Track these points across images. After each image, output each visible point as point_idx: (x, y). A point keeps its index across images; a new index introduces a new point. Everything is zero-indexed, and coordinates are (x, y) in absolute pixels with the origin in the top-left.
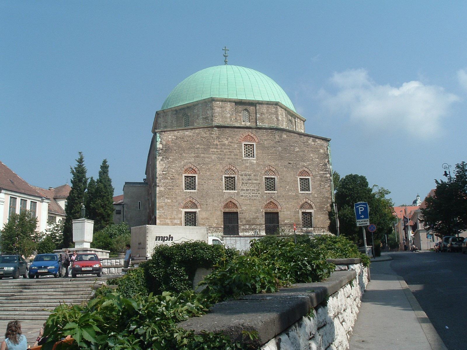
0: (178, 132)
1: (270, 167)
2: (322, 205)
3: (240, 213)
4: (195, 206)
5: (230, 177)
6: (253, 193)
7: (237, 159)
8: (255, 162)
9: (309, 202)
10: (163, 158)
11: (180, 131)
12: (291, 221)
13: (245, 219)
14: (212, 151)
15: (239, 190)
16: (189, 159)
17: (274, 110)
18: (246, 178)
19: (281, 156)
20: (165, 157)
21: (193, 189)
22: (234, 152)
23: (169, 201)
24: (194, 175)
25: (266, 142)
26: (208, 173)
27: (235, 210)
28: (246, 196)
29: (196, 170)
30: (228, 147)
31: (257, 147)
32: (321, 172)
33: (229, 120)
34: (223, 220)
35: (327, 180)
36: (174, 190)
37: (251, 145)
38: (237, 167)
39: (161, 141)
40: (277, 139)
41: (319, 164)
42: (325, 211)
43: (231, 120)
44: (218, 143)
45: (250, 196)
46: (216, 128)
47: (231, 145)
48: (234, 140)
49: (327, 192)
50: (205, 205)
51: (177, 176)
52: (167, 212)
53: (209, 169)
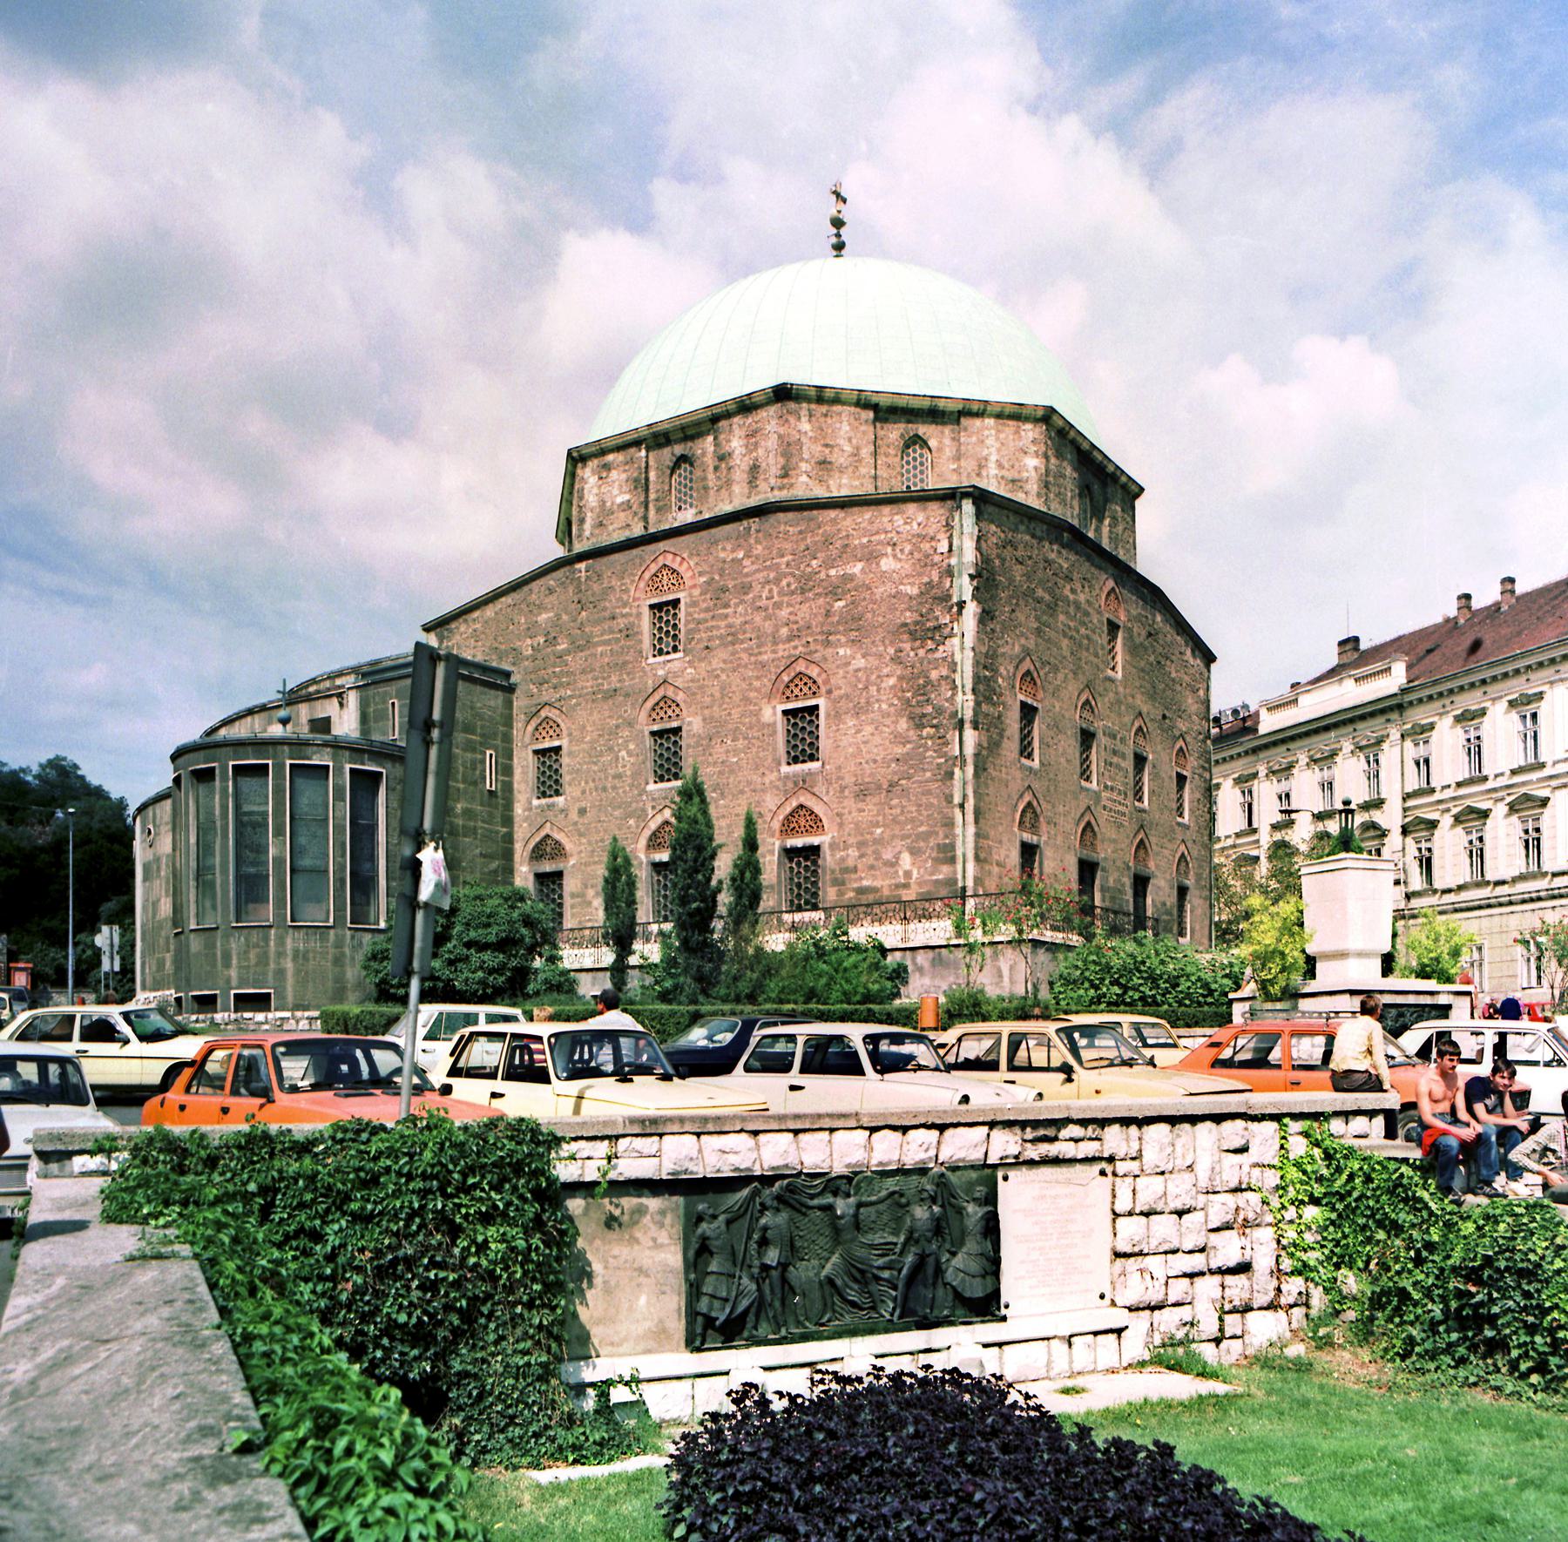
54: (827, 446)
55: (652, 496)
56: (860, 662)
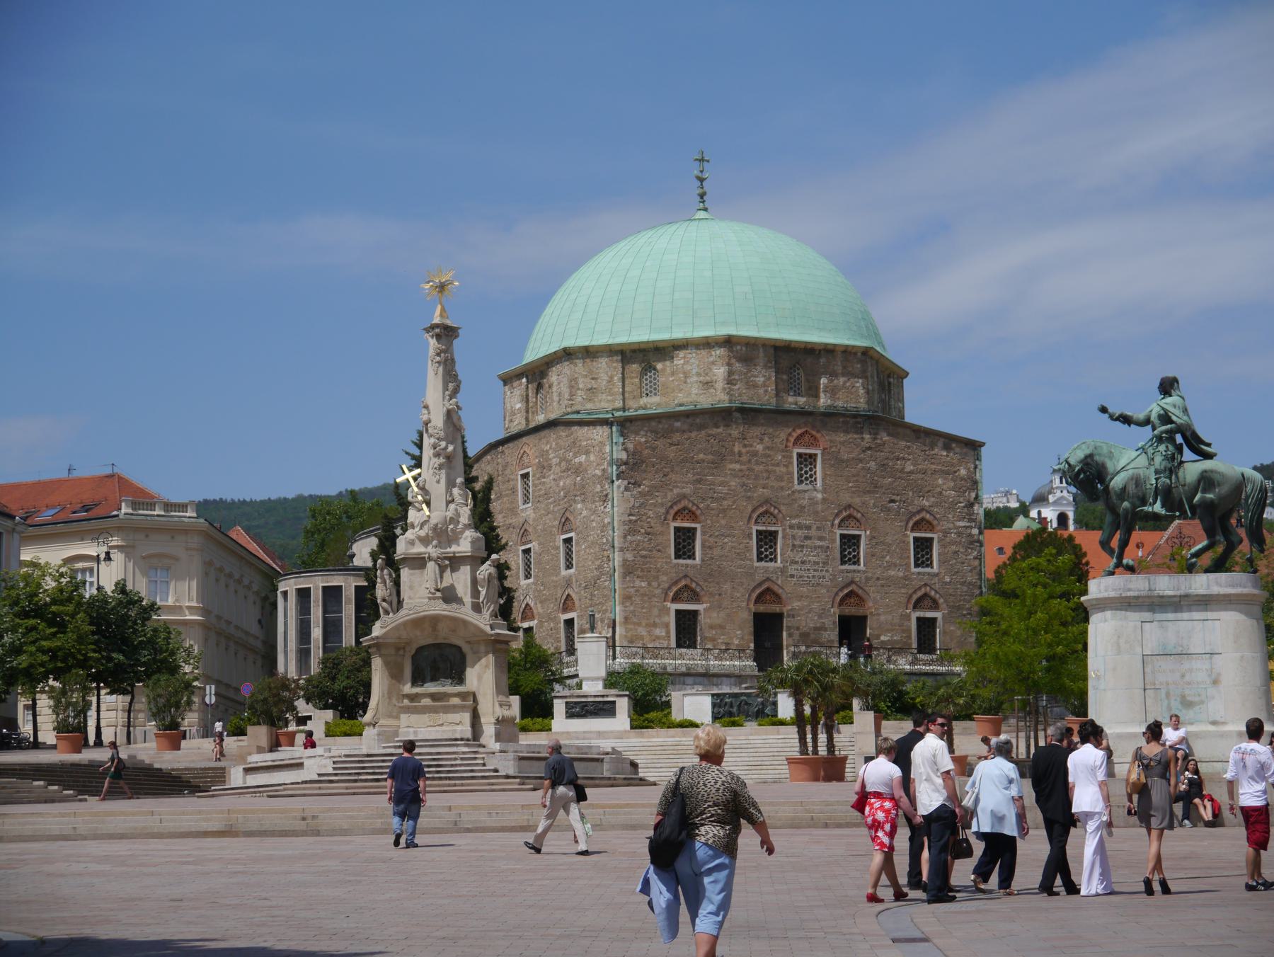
0: (660, 422)
1: (852, 509)
2: (960, 600)
3: (789, 616)
4: (695, 597)
5: (766, 531)
6: (815, 570)
7: (782, 488)
8: (819, 496)
9: (933, 593)
10: (629, 483)
11: (664, 421)
12: (892, 637)
13: (798, 629)
14: (730, 469)
15: (787, 562)
16: (683, 485)
17: (859, 366)
18: (800, 533)
19: (874, 482)
20: (633, 481)
21: (689, 557)
22: (775, 472)
23: (643, 584)
24: (693, 525)
25: (843, 447)
26: (723, 522)
27: (775, 608)
28: (801, 577)
29: (698, 512)
30: (764, 460)
31: (823, 461)
32: (961, 524)
33: (761, 391)
34: (752, 629)
35: (972, 543)
36: (653, 560)
37: (811, 456)
38: (783, 508)
39: (623, 444)
40: (866, 440)
41: (957, 504)
42: (964, 615)
43: (766, 391)
44: (744, 450)
45: (809, 578)
46: (739, 412)
47: (769, 456)
48: (776, 443)
49: (971, 571)
50: (717, 597)
51: (658, 528)
52: (640, 610)
53: (724, 511)
54: (593, 379)
55: (531, 405)
56: (585, 513)
